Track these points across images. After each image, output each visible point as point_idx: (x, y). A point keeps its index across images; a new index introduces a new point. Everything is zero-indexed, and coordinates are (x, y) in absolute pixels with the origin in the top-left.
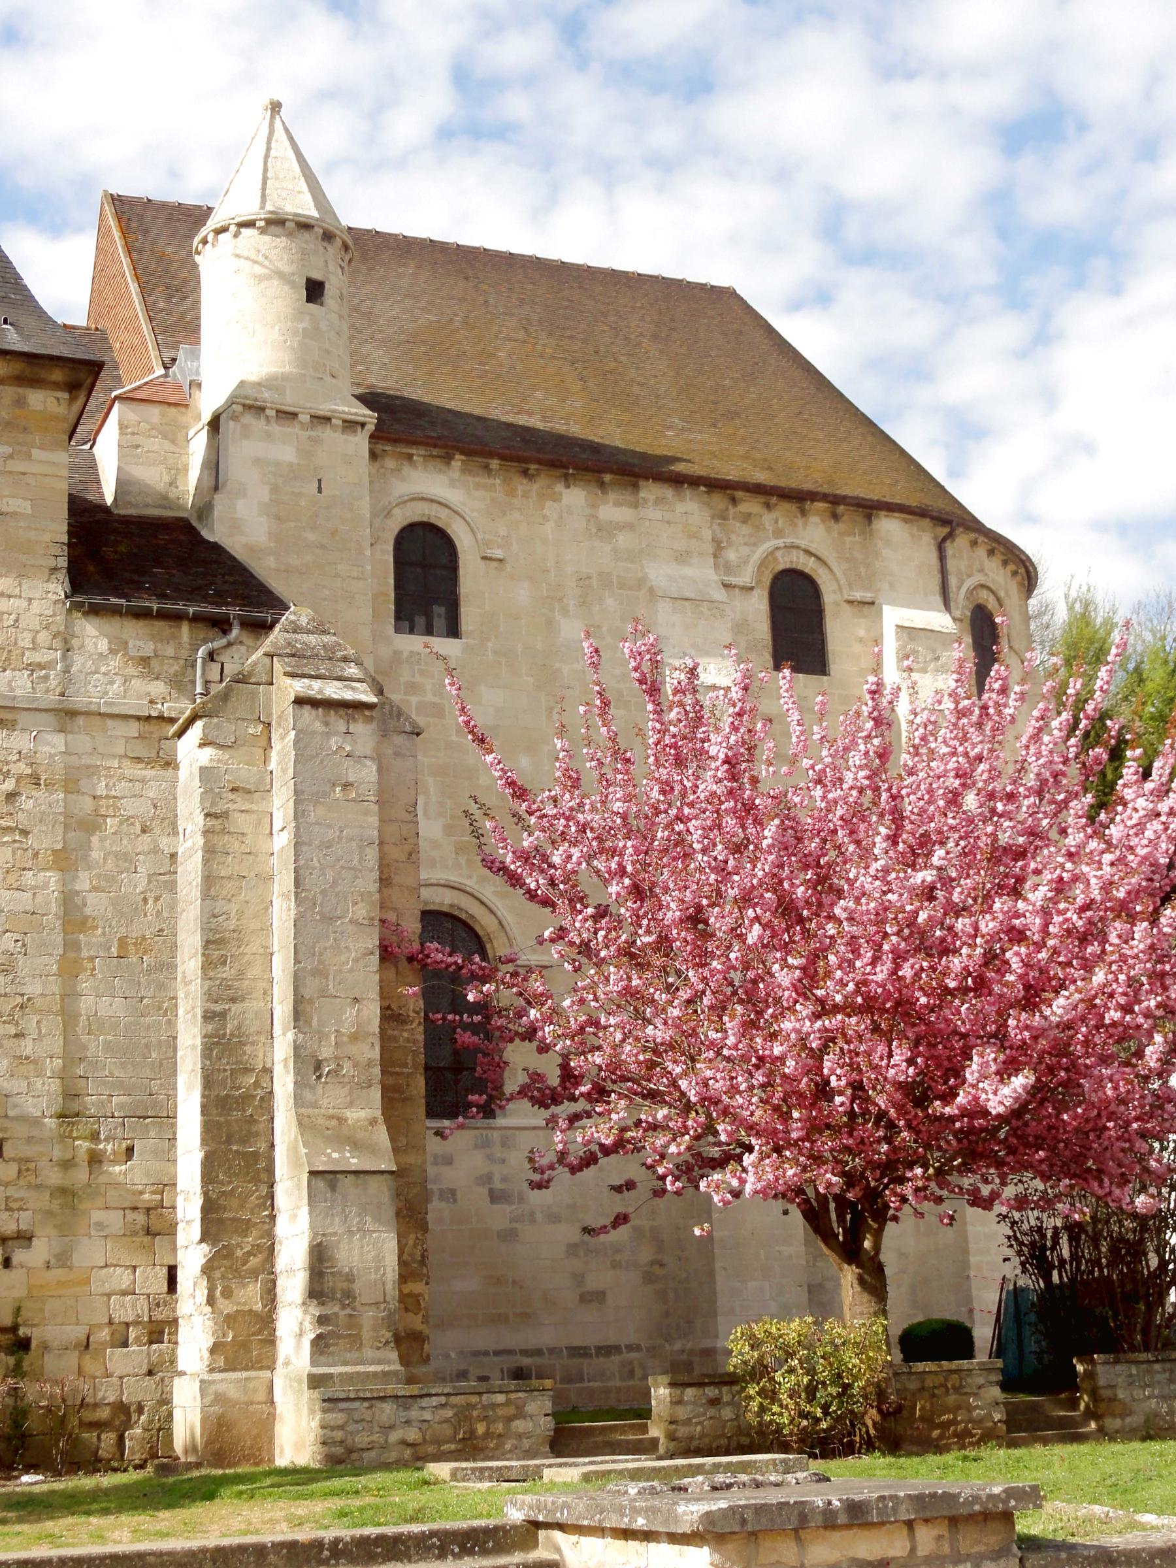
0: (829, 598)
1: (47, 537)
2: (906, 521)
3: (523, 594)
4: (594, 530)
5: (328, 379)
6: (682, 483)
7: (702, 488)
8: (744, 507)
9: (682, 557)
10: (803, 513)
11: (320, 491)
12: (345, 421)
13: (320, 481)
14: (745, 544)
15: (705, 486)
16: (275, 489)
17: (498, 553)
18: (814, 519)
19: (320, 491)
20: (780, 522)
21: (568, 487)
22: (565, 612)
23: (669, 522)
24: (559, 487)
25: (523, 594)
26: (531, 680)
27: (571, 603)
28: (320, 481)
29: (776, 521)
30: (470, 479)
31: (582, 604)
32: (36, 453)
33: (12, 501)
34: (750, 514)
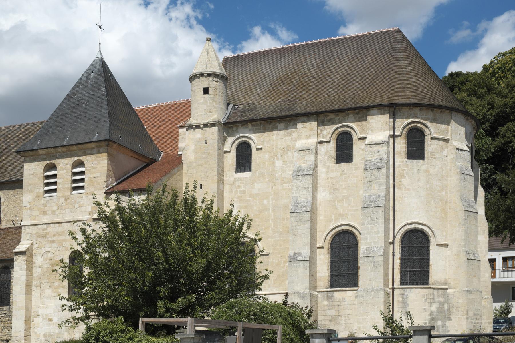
0: (355, 138)
1: (103, 180)
2: (379, 109)
3: (267, 156)
4: (286, 134)
5: (209, 113)
6: (309, 115)
7: (315, 115)
8: (329, 117)
9: (308, 137)
10: (348, 115)
11: (206, 143)
12: (211, 124)
13: (206, 141)
14: (329, 128)
15: (315, 114)
16: (196, 145)
17: (260, 147)
18: (351, 115)
19: (206, 143)
20: (340, 119)
21: (279, 124)
22: (277, 159)
23: (305, 128)
24: (277, 124)
25: (267, 156)
26: (268, 179)
27: (279, 156)
28: (206, 141)
29: (339, 119)
30: (254, 128)
31: (282, 156)
32: (102, 162)
33: (97, 174)
34: (331, 119)
